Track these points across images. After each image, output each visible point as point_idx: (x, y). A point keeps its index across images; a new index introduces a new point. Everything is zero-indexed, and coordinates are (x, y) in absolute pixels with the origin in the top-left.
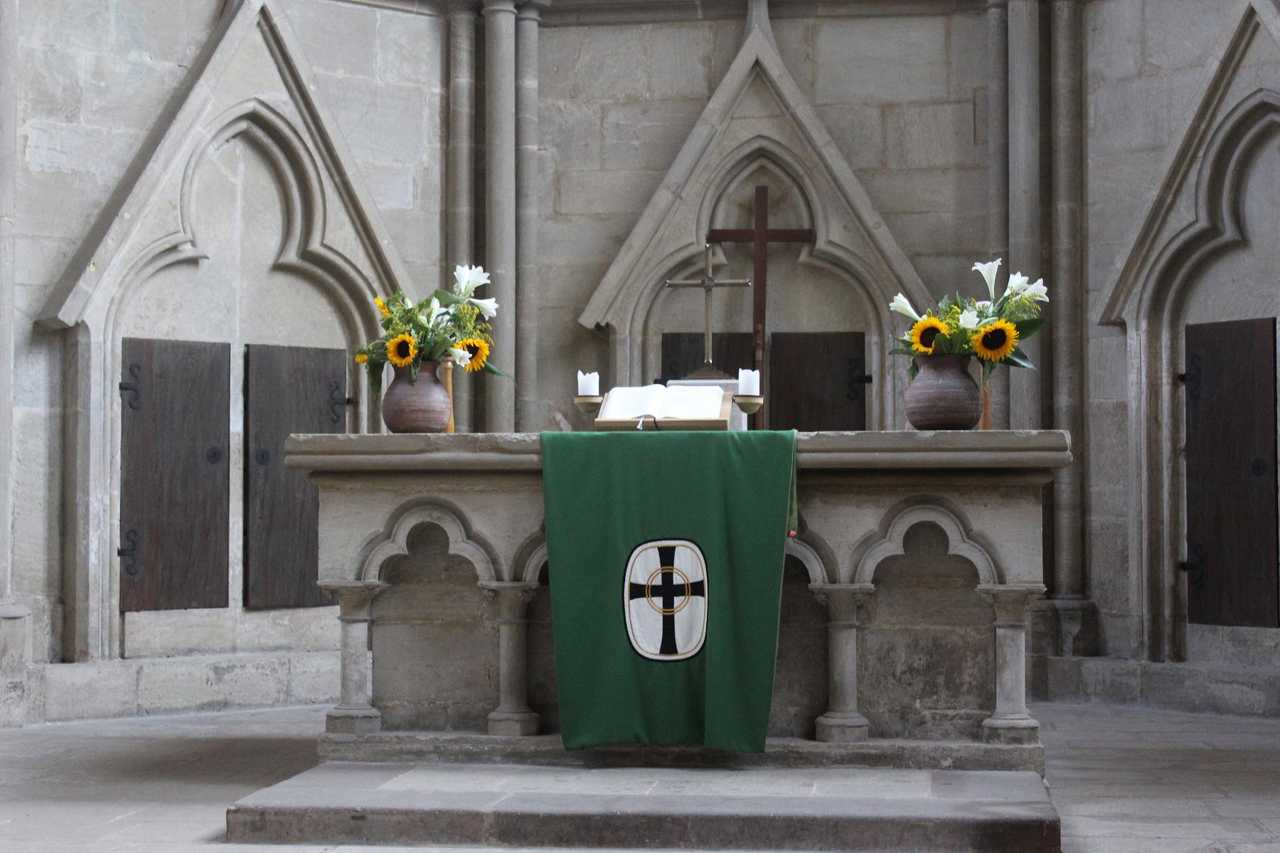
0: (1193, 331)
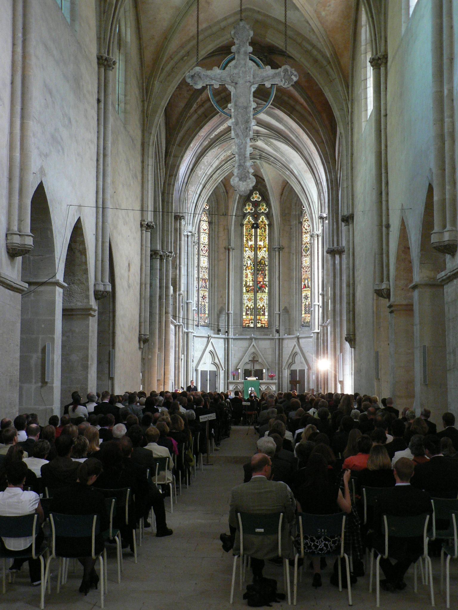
0: (291, 371)
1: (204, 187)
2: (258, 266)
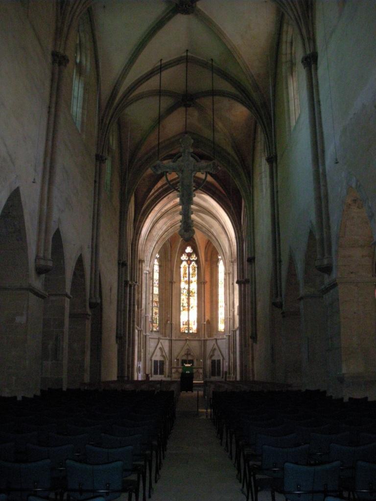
1: (157, 243)
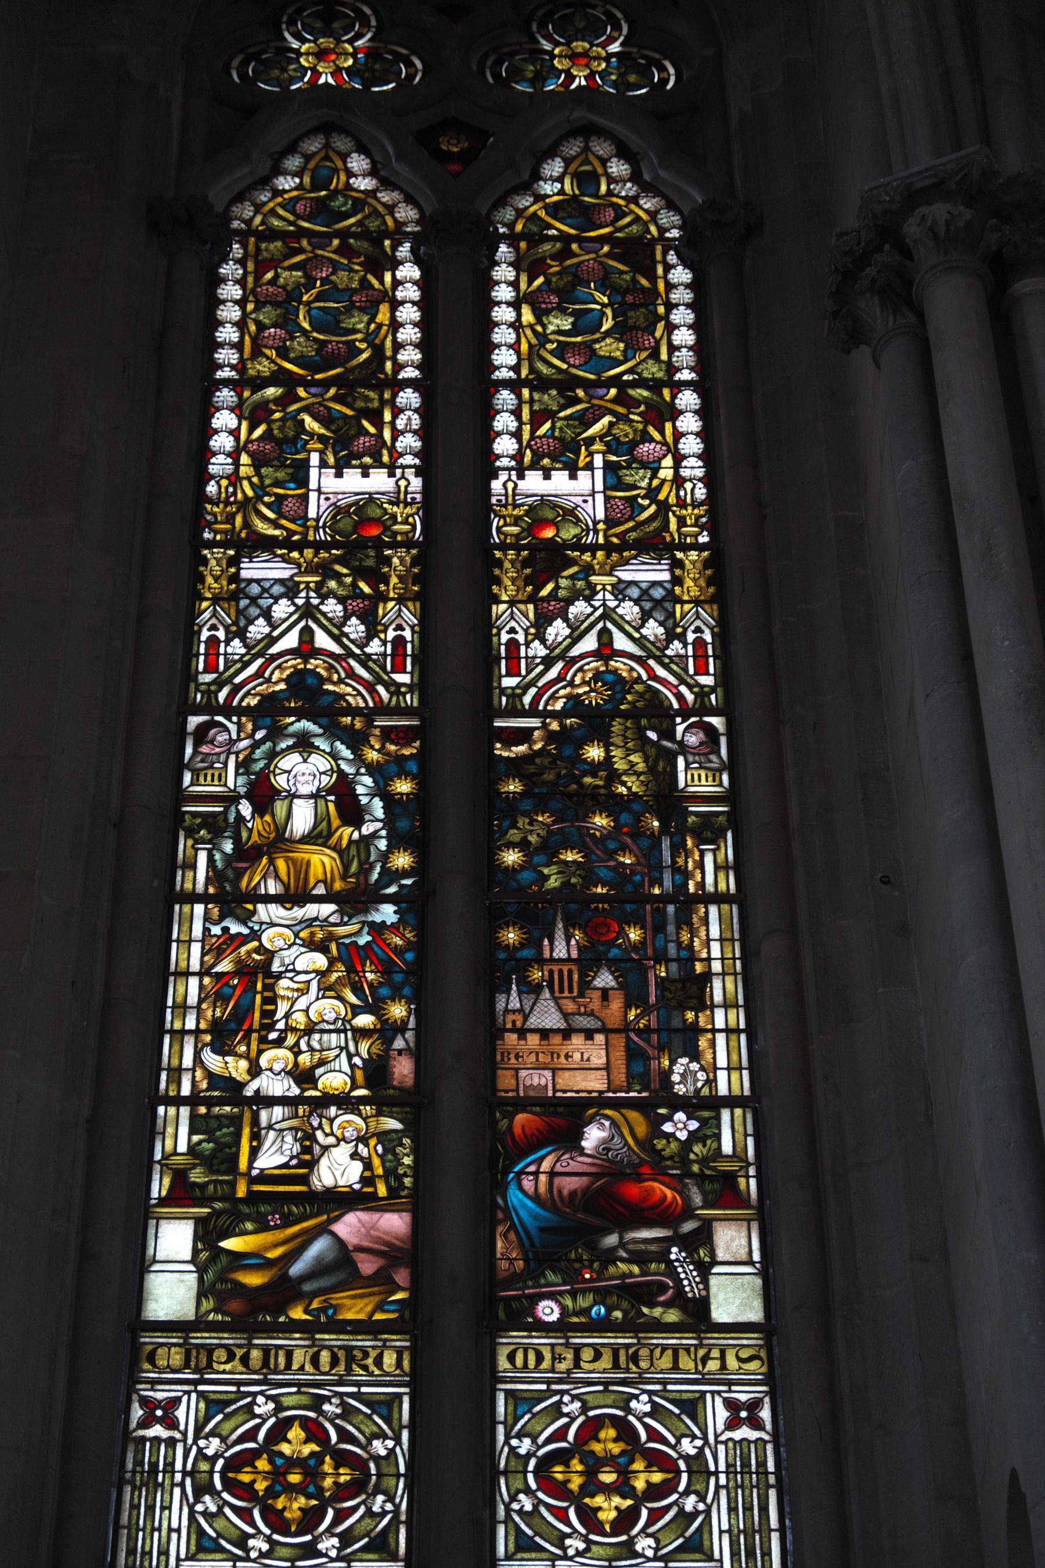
2: (490, 854)
